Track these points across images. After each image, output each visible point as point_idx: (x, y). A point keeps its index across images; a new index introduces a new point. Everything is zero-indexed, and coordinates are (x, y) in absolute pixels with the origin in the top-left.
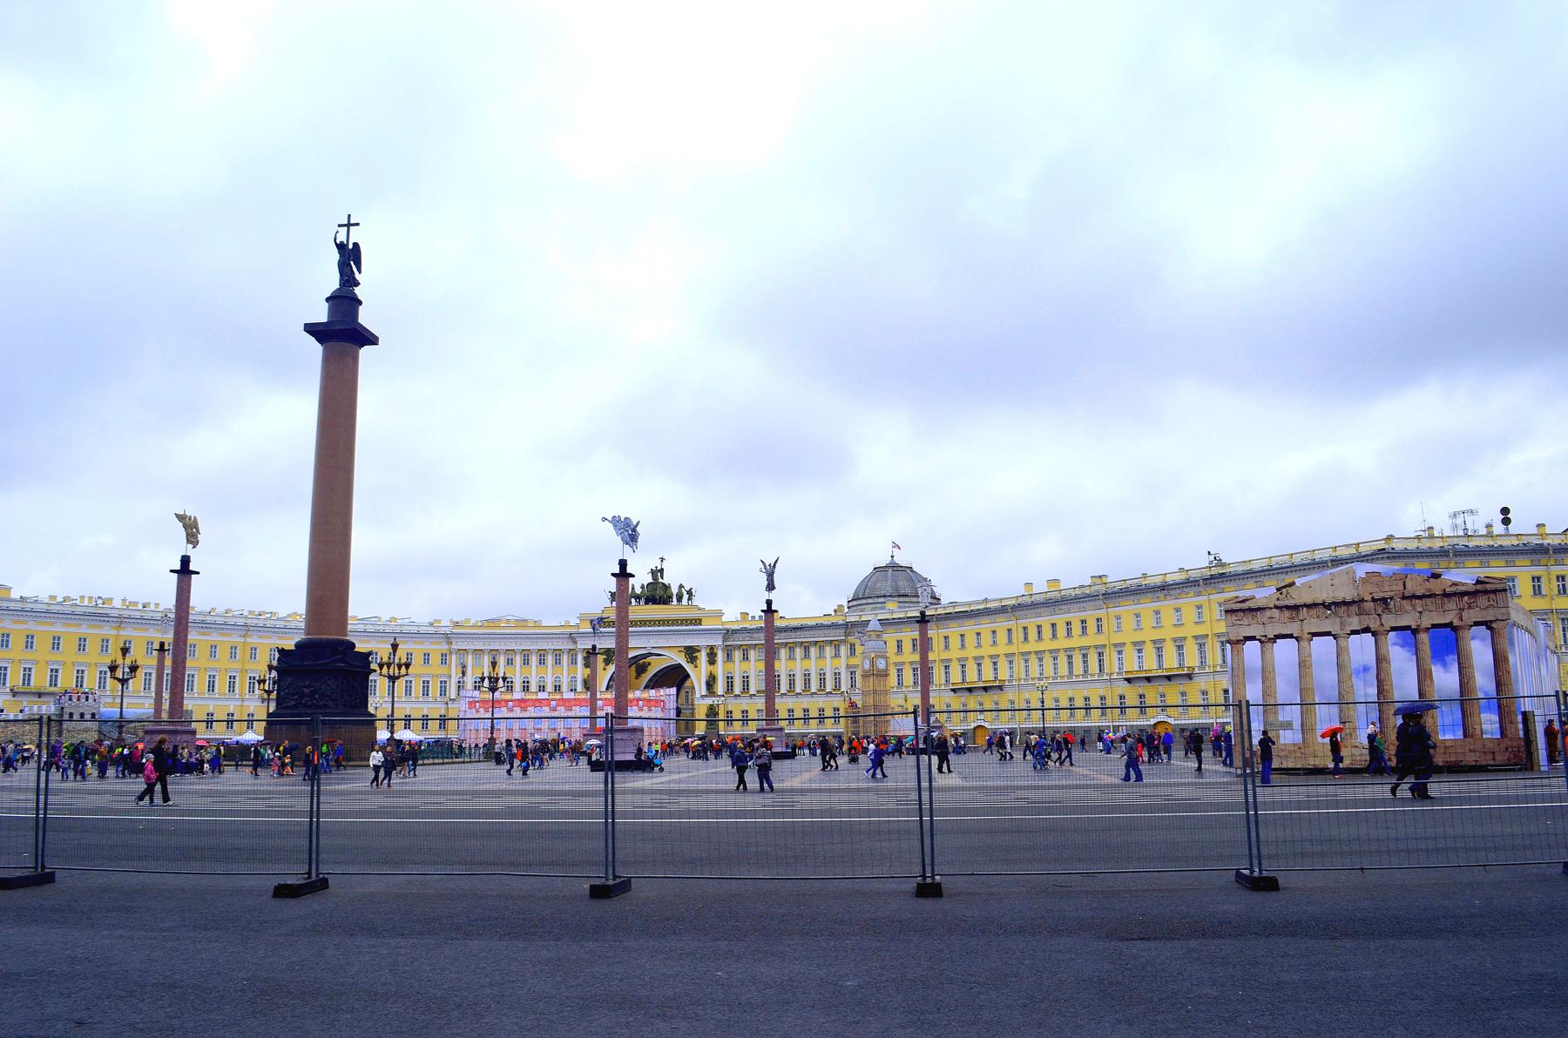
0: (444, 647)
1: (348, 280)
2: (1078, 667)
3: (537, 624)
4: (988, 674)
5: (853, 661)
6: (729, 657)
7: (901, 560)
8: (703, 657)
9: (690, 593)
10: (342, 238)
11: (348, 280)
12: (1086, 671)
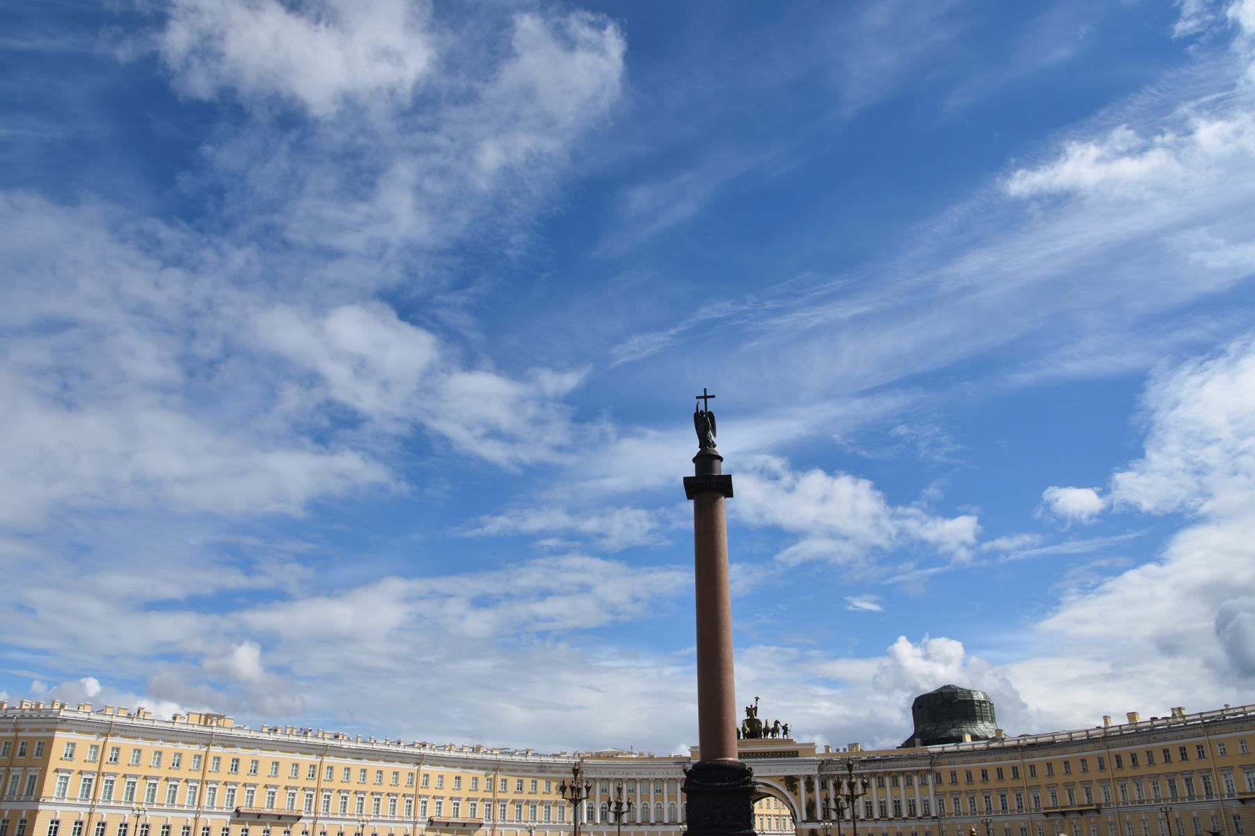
1: (705, 443)
2: (1182, 789)
4: (1081, 798)
5: (940, 789)
6: (824, 786)
8: (802, 785)
9: (785, 728)
10: (702, 408)
11: (705, 443)
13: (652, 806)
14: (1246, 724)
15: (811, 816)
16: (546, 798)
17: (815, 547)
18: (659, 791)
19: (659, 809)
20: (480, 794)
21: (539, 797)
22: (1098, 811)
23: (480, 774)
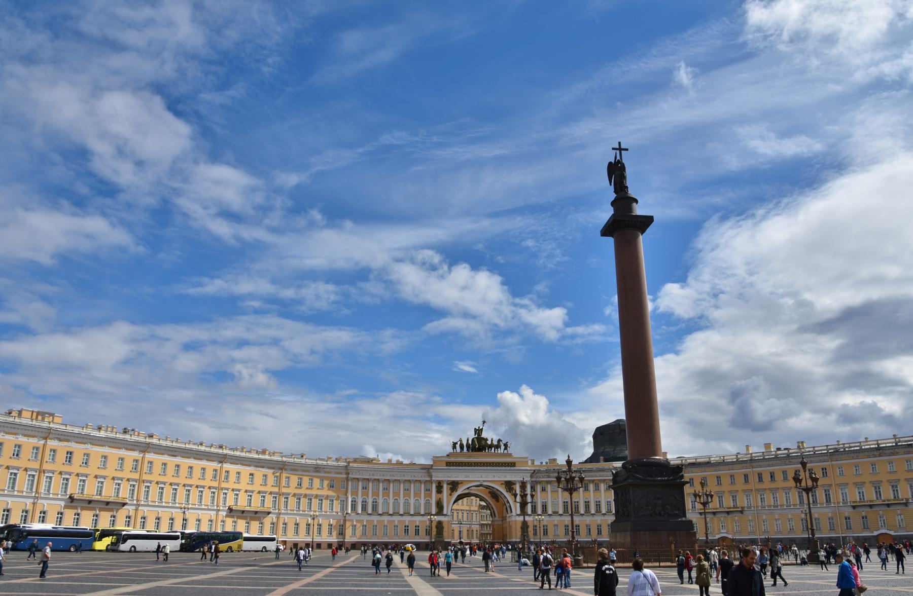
0: (345, 476)
4: (728, 503)
9: (506, 445)
13: (402, 501)
14: (861, 454)
15: (523, 512)
16: (320, 493)
17: (456, 323)
18: (407, 490)
19: (407, 504)
20: (269, 489)
21: (314, 492)
22: (741, 512)
23: (269, 472)
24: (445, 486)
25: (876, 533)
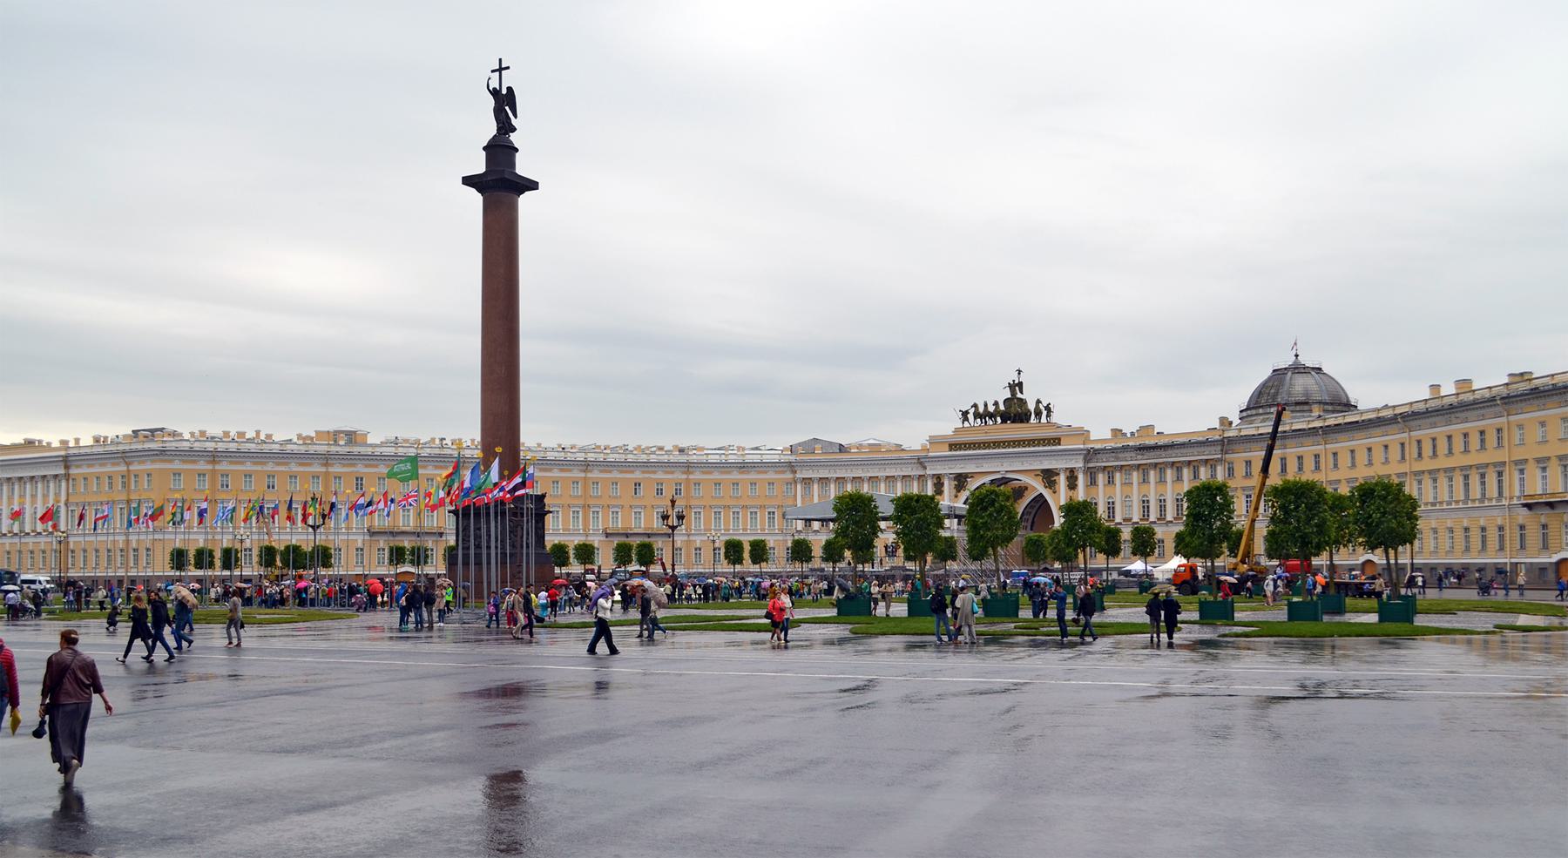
2: (1476, 491)
3: (899, 448)
7: (1307, 360)
8: (1062, 480)
9: (1048, 408)
10: (494, 84)
11: (505, 127)
12: (1484, 495)
24: (946, 483)
25: (1555, 558)
